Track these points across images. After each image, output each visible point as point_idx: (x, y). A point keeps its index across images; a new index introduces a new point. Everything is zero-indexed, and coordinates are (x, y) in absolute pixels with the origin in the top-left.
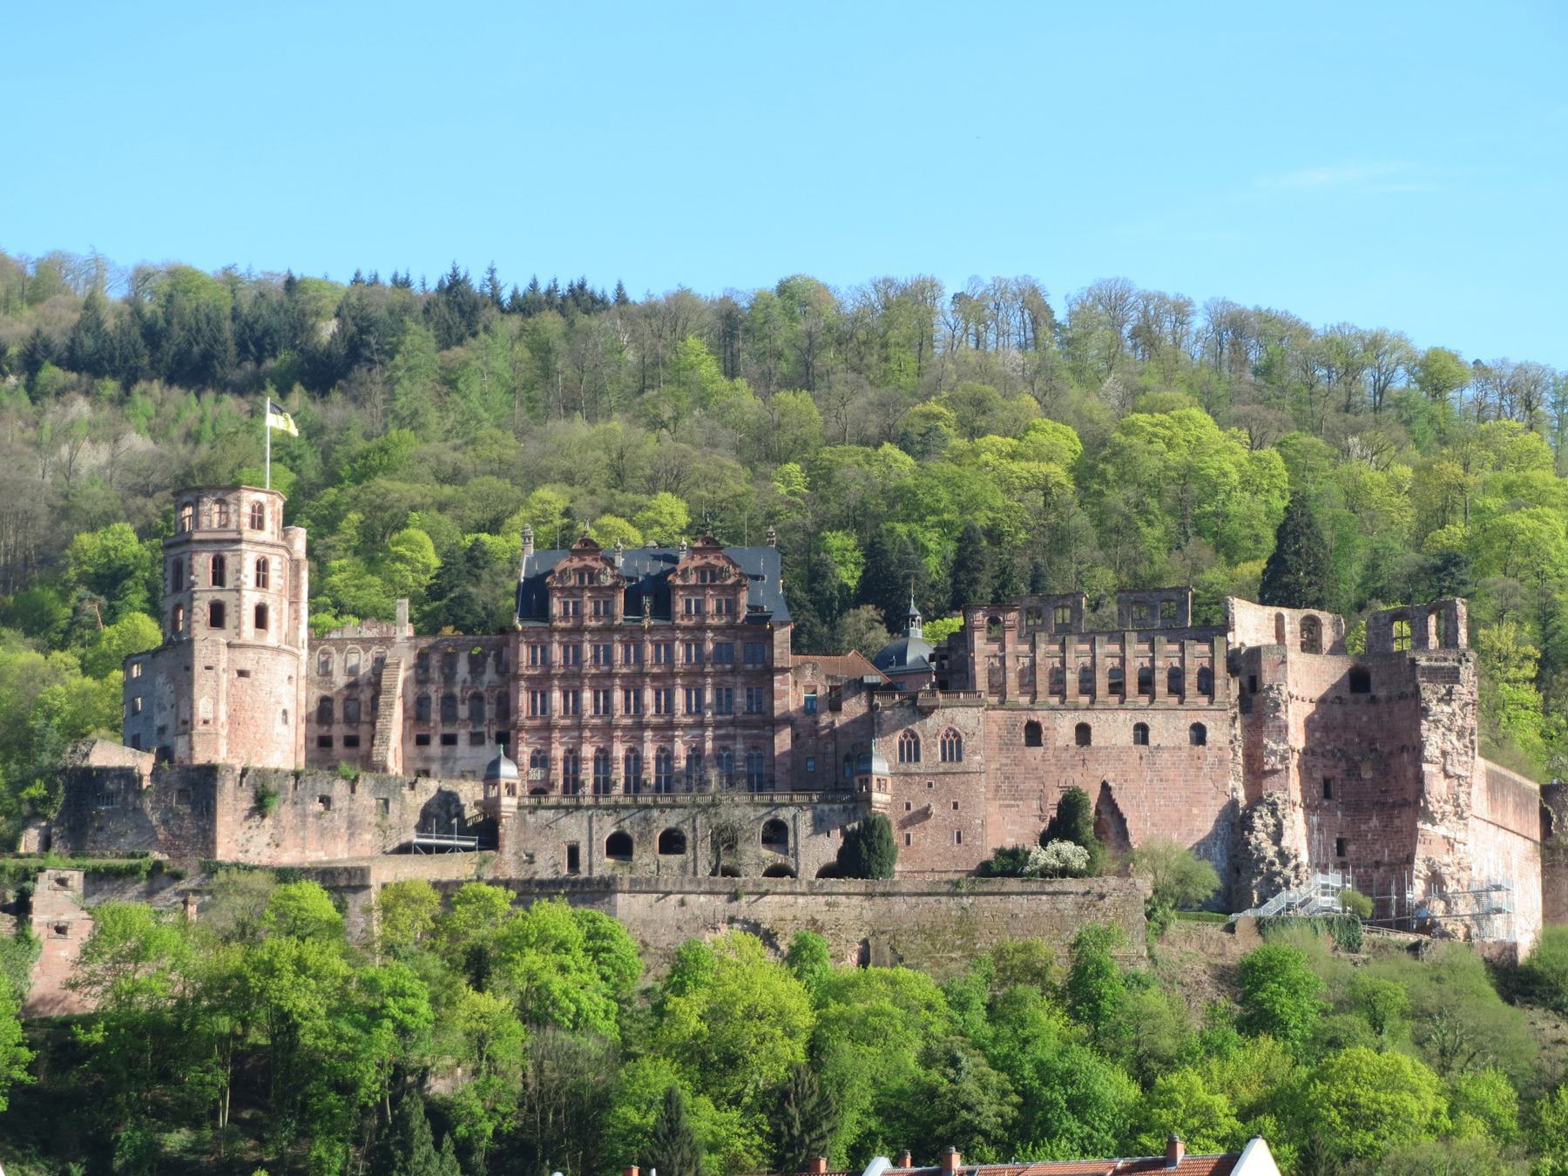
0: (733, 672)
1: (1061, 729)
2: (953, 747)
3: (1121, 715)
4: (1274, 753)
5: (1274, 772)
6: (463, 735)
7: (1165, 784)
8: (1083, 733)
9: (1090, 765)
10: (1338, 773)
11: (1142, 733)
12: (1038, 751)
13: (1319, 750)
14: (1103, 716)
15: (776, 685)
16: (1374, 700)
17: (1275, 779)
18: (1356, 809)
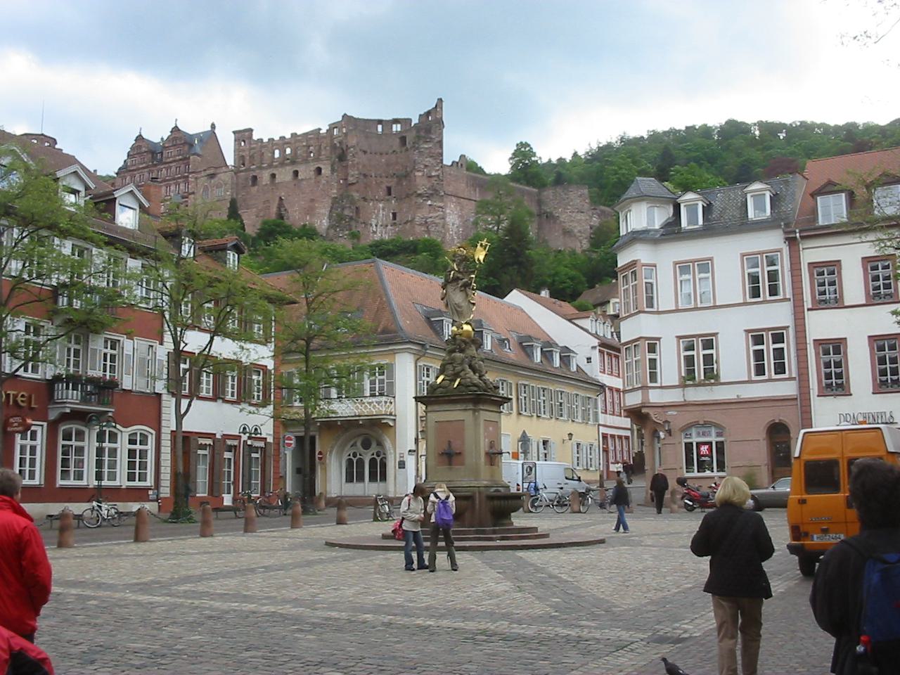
0: (179, 178)
1: (265, 177)
3: (288, 168)
4: (353, 176)
5: (353, 184)
7: (304, 195)
8: (273, 176)
9: (275, 190)
10: (392, 183)
11: (296, 173)
12: (256, 187)
13: (384, 175)
14: (280, 169)
15: (190, 179)
16: (407, 150)
17: (353, 187)
18: (399, 199)
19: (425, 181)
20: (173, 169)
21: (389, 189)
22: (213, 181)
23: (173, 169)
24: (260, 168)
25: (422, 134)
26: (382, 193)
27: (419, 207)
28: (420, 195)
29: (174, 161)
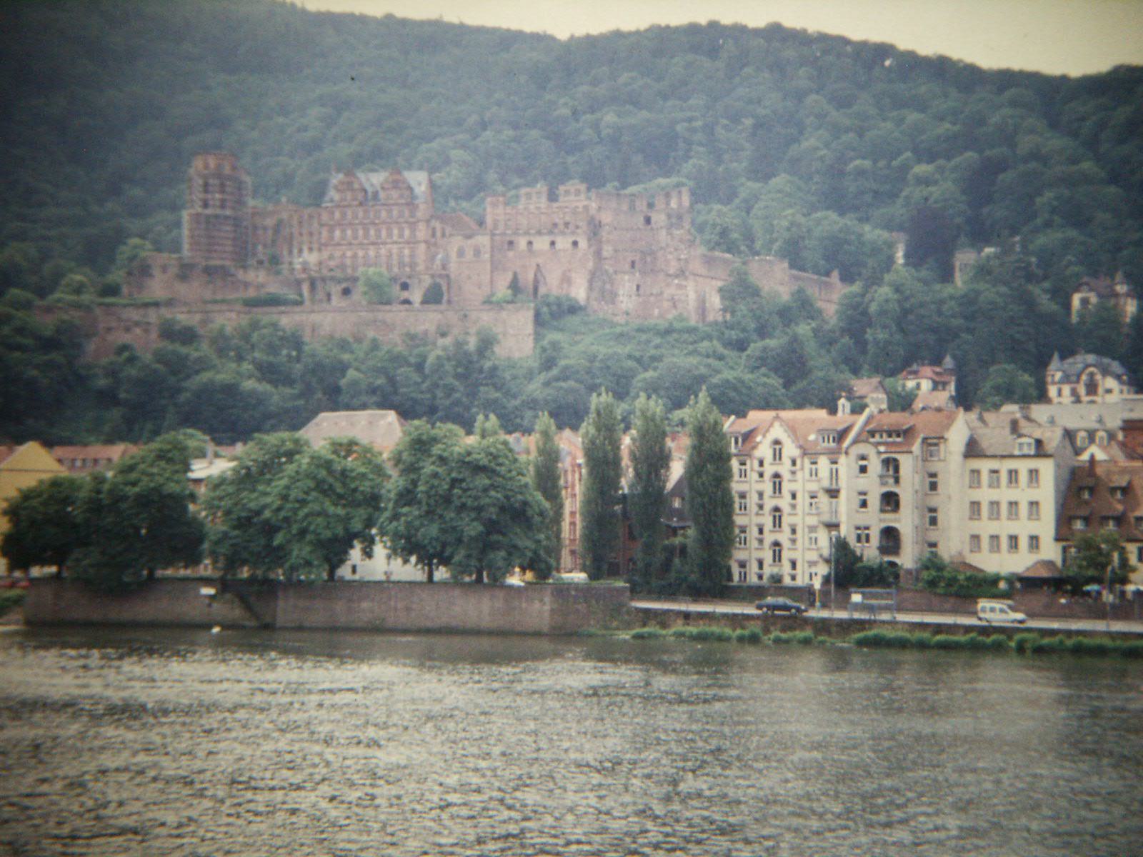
1: (522, 243)
2: (477, 252)
6: (305, 248)
8: (530, 243)
10: (637, 258)
11: (553, 243)
18: (643, 273)
19: (674, 263)
20: (395, 213)
21: (633, 264)
22: (469, 242)
23: (395, 213)
24: (518, 234)
25: (674, 220)
26: (627, 267)
27: (668, 285)
28: (669, 275)
29: (396, 204)
